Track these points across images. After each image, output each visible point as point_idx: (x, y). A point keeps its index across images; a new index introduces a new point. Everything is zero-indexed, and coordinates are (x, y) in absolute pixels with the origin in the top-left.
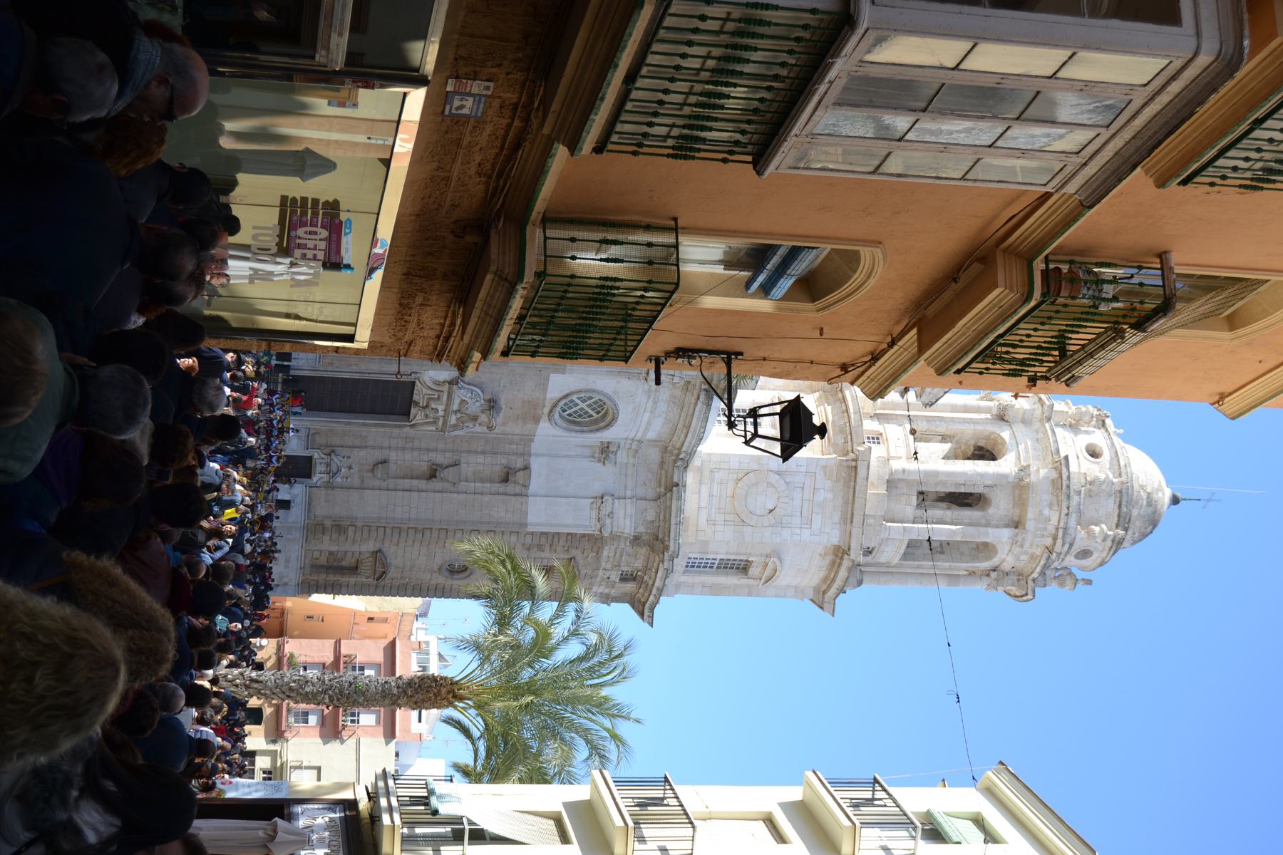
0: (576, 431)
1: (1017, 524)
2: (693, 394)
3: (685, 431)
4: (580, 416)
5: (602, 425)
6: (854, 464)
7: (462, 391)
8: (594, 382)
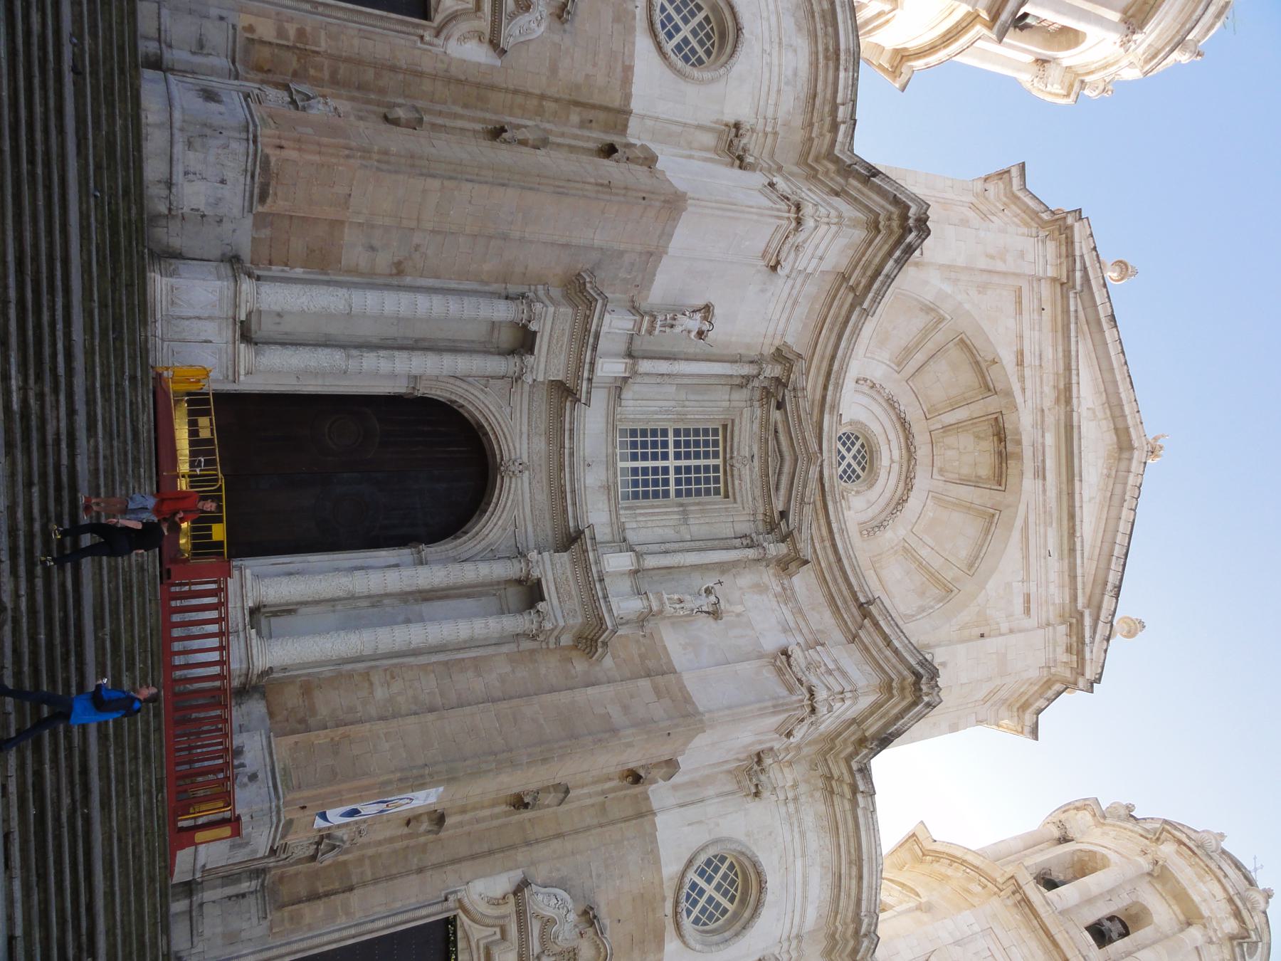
0: (717, 944)
1: (1191, 917)
2: (843, 796)
3: (854, 871)
4: (710, 917)
5: (747, 914)
6: (1018, 897)
7: (540, 897)
8: (718, 825)
